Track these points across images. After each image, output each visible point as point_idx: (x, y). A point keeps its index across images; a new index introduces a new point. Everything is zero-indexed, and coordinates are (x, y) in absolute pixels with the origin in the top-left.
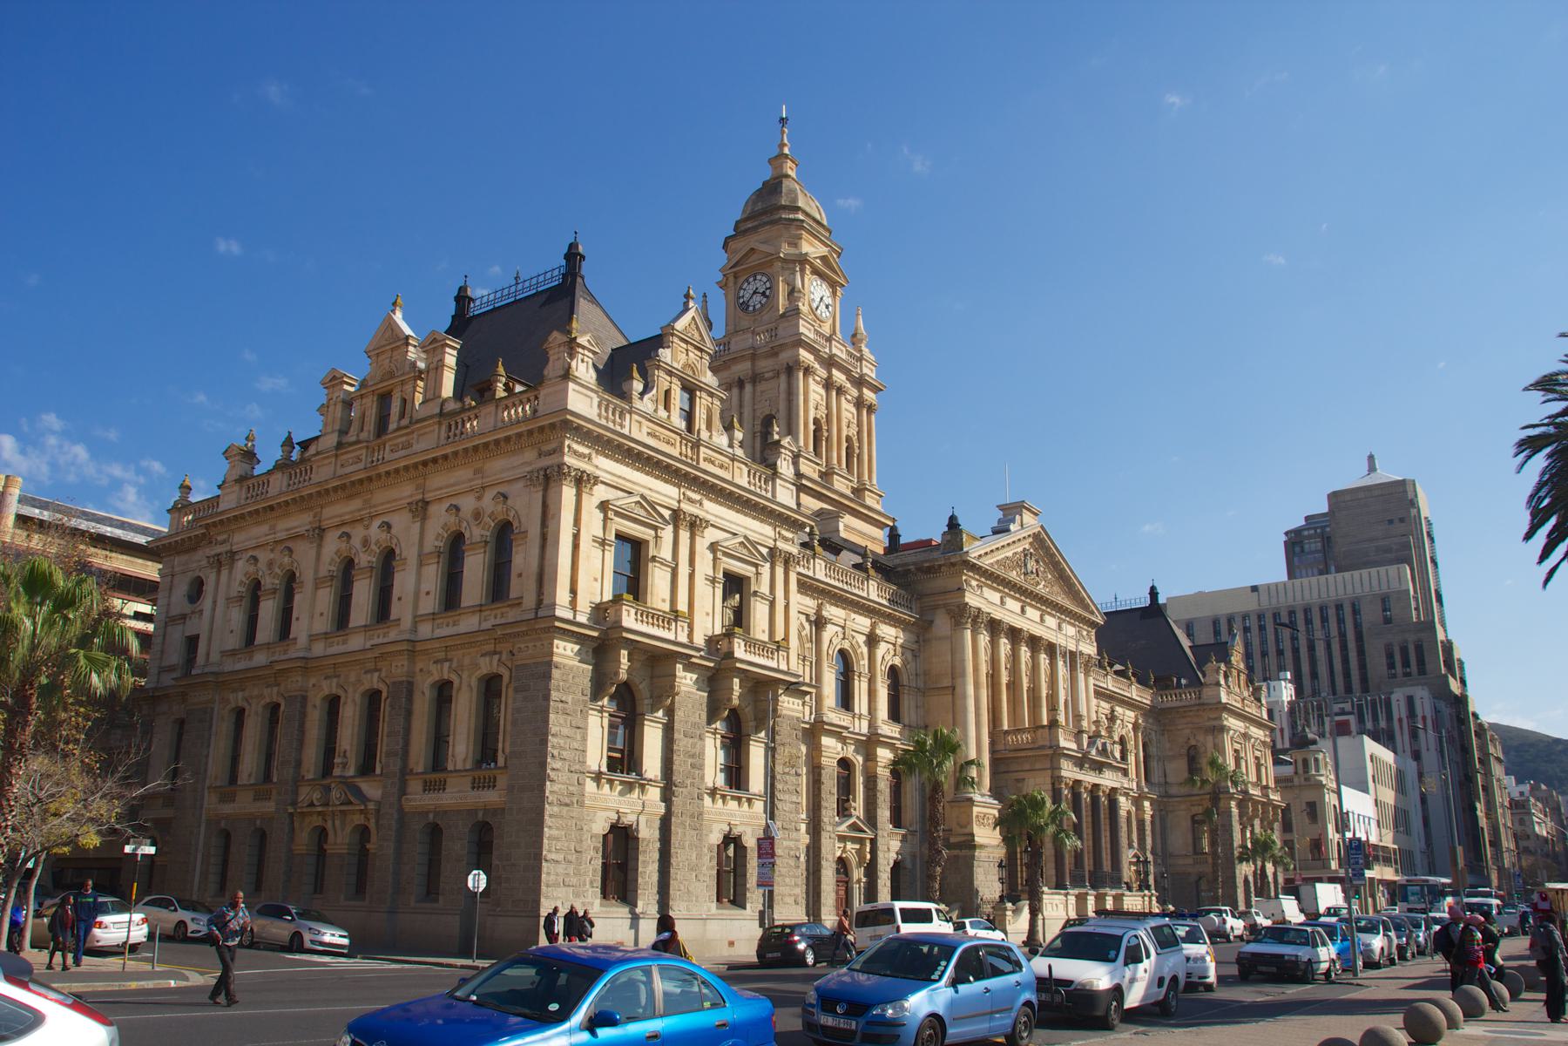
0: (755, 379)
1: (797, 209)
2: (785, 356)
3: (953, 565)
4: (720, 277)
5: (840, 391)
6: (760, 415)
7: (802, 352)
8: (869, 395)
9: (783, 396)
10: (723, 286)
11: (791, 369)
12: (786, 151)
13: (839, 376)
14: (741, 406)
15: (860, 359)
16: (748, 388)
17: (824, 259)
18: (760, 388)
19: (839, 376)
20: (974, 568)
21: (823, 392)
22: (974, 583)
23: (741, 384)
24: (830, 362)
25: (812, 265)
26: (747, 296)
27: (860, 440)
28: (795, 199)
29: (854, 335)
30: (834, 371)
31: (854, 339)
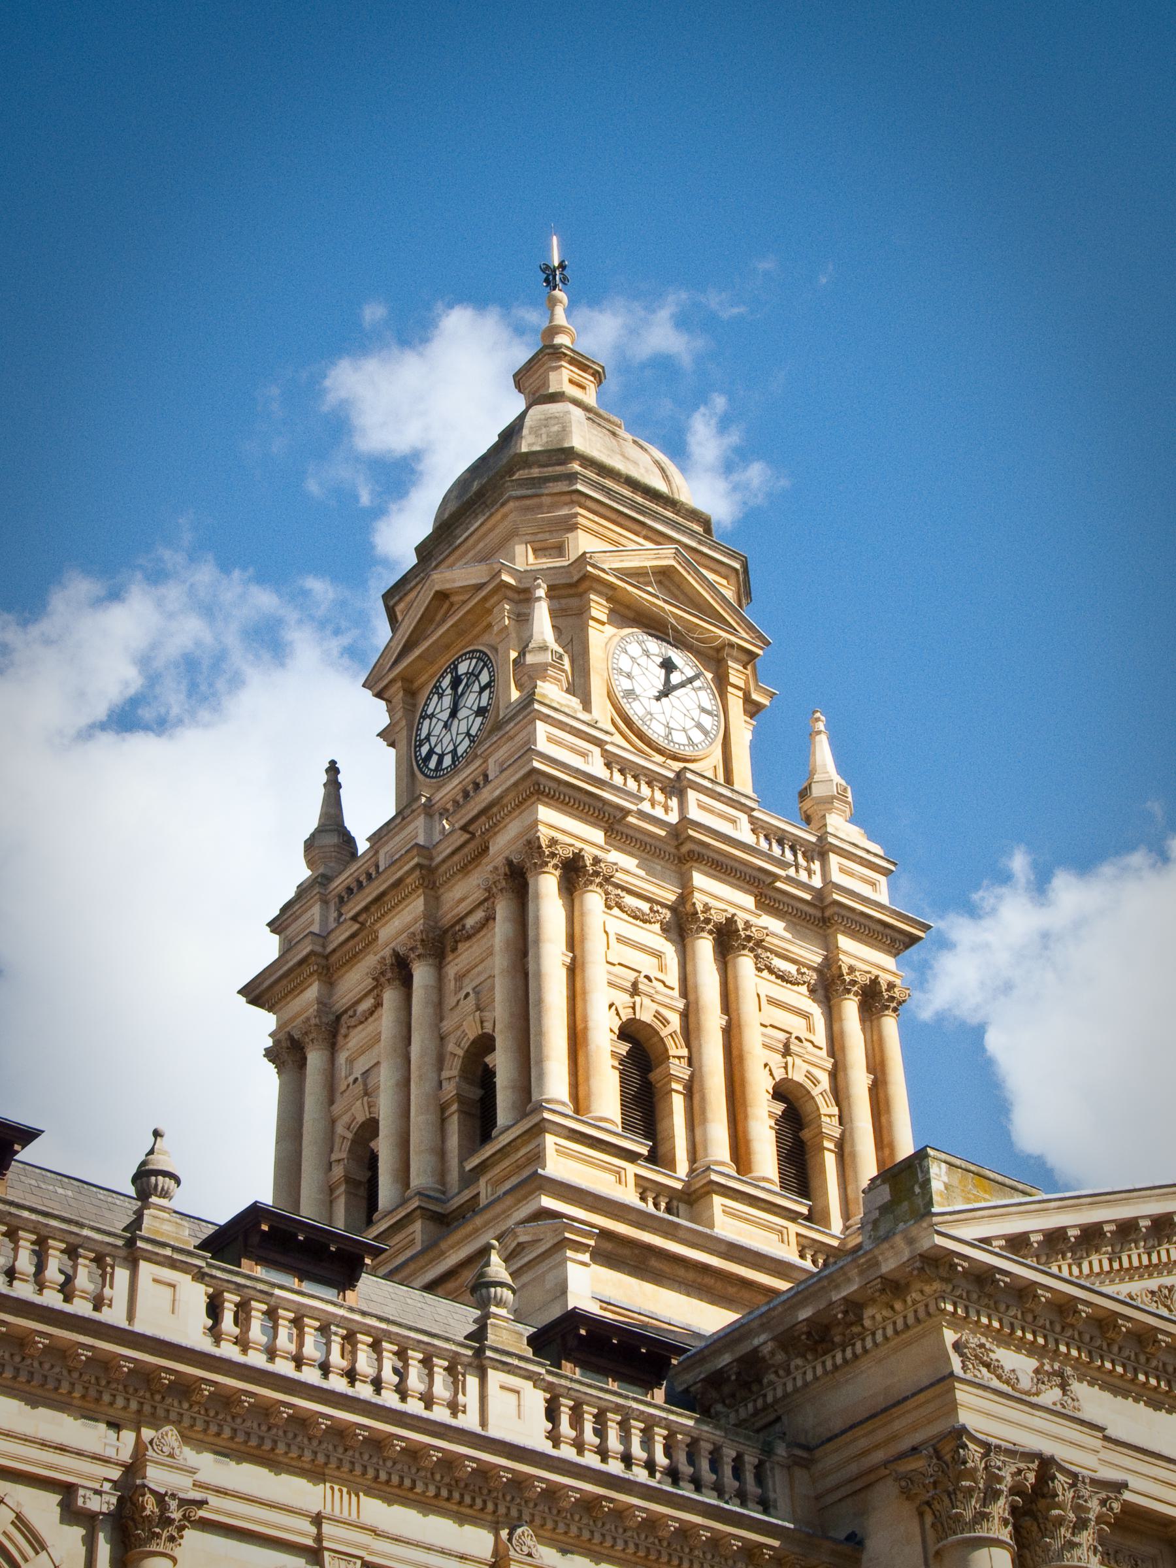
0: (440, 942)
2: (504, 844)
3: (894, 1287)
5: (728, 939)
6: (456, 1049)
8: (859, 956)
11: (518, 881)
12: (561, 339)
15: (820, 851)
16: (421, 974)
17: (665, 576)
18: (451, 971)
24: (681, 851)
25: (612, 594)
27: (839, 1092)
28: (565, 430)
29: (804, 794)
30: (699, 879)
31: (805, 802)
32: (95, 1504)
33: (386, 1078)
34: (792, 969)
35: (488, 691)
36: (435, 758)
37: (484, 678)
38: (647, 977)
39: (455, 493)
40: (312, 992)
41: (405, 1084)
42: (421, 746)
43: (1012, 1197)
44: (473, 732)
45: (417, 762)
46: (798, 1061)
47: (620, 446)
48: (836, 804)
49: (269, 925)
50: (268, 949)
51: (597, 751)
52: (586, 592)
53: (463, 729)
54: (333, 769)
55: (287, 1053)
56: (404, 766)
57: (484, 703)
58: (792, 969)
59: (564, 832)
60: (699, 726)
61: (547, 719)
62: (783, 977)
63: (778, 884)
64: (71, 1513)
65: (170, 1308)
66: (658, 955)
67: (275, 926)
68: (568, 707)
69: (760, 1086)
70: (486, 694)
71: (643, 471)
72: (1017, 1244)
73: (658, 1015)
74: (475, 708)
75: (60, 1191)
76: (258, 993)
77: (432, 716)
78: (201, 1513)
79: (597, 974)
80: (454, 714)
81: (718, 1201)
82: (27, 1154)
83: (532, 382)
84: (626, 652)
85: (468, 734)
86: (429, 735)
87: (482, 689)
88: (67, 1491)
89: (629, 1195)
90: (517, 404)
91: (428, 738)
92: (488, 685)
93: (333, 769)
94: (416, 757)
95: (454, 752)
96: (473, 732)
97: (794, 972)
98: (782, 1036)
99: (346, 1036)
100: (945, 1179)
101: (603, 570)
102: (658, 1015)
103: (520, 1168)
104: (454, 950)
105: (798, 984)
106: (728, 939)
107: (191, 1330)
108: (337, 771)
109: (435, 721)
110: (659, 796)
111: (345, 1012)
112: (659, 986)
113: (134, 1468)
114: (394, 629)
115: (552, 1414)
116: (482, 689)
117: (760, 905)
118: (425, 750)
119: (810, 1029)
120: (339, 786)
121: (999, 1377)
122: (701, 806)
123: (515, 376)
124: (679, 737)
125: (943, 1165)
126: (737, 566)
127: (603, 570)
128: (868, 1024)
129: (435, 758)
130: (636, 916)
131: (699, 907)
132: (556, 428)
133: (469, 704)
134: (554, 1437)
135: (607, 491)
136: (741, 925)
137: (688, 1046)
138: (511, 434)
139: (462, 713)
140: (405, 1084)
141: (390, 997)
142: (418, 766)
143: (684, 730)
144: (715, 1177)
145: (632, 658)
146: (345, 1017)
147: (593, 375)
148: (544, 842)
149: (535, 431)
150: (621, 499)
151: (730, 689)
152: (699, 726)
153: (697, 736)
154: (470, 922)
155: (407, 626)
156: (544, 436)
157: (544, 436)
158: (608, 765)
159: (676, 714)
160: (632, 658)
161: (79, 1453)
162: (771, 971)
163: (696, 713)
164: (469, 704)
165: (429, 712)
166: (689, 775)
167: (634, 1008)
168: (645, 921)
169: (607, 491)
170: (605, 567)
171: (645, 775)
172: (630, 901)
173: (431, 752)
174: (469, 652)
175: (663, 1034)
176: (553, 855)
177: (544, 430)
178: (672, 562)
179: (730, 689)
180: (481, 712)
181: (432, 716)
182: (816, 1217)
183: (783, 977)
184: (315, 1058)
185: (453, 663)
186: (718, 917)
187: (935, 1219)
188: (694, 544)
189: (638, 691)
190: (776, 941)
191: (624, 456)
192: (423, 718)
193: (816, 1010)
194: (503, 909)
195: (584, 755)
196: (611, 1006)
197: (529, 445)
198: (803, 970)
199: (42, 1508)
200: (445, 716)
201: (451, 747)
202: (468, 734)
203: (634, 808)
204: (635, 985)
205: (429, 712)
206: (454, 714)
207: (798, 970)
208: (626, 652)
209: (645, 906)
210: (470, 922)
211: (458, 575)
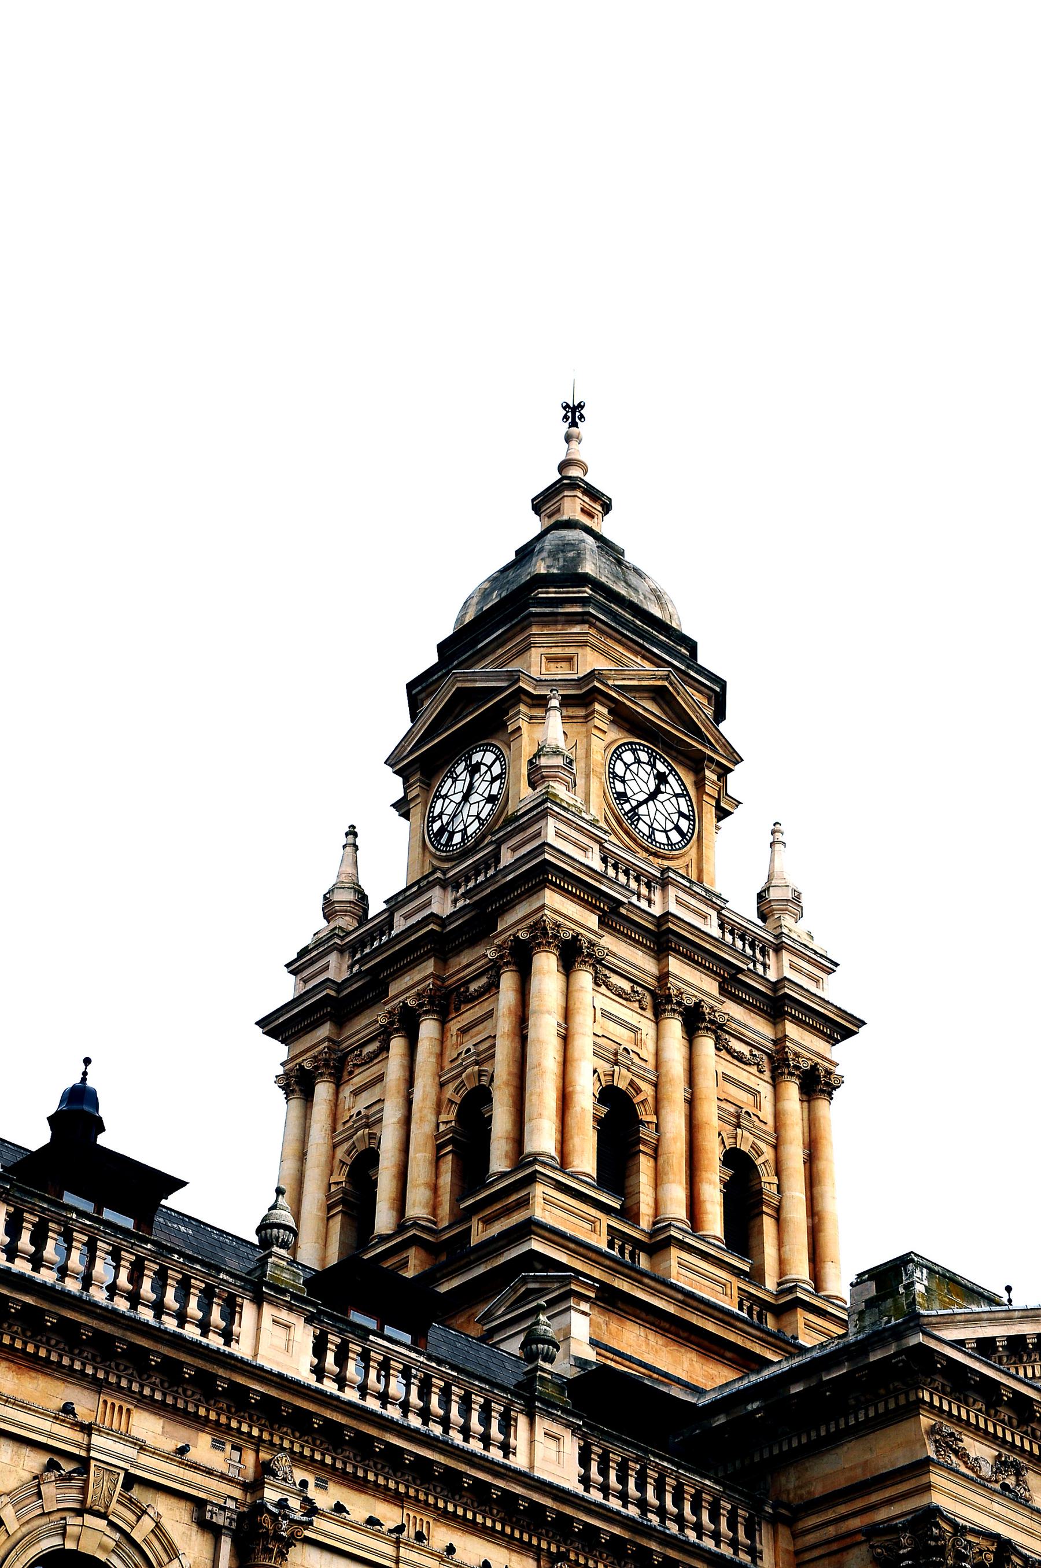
0: (445, 1002)
1: (585, 579)
2: (513, 922)
4: (395, 788)
7: (552, 899)
9: (504, 1025)
10: (402, 807)
13: (691, 980)
14: (410, 1082)
16: (428, 1029)
17: (660, 695)
18: (454, 1026)
19: (691, 980)
20: (959, 1381)
21: (647, 1027)
22: (978, 1449)
23: (407, 1024)
26: (449, 810)
28: (578, 559)
30: (675, 965)
32: (220, 1520)
33: (392, 1114)
34: (745, 1050)
35: (499, 781)
36: (446, 834)
37: (496, 770)
38: (625, 1049)
39: (475, 600)
40: (325, 1031)
41: (407, 1121)
42: (434, 821)
43: (979, 1305)
44: (483, 816)
45: (429, 836)
46: (746, 1134)
47: (623, 573)
48: (791, 907)
49: (287, 966)
50: (283, 989)
51: (596, 847)
52: (591, 703)
53: (474, 811)
54: (352, 832)
55: (298, 1083)
56: (419, 836)
57: (494, 792)
58: (745, 1050)
59: (565, 916)
60: (677, 828)
61: (557, 816)
62: (739, 1058)
63: (740, 976)
64: (205, 1525)
65: (278, 1343)
66: (635, 1030)
67: (295, 968)
68: (575, 806)
69: (713, 1152)
70: (496, 785)
71: (641, 597)
72: (985, 1347)
73: (632, 1083)
74: (486, 795)
75: (183, 1229)
76: (278, 1025)
77: (445, 797)
78: (307, 1533)
79: (584, 1045)
80: (466, 798)
81: (675, 1253)
82: (174, 1201)
83: (549, 507)
84: (622, 760)
85: (478, 817)
86: (441, 813)
87: (494, 780)
88: (199, 1504)
89: (601, 1242)
90: (534, 526)
91: (440, 816)
92: (499, 777)
93: (352, 832)
94: (428, 831)
95: (464, 831)
96: (483, 816)
97: (747, 1053)
98: (732, 1109)
99: (351, 1073)
100: (926, 1283)
101: (607, 685)
102: (632, 1083)
103: (508, 1211)
104: (457, 1009)
105: (750, 1064)
106: (695, 1021)
107: (299, 1366)
108: (355, 835)
109: (447, 801)
110: (644, 891)
111: (353, 1051)
112: (636, 1060)
113: (254, 1487)
114: (414, 716)
115: (584, 1460)
116: (494, 780)
117: (722, 991)
118: (437, 826)
119: (758, 1105)
120: (356, 847)
121: (965, 1463)
122: (679, 902)
123: (533, 500)
124: (661, 837)
125: (925, 1270)
126: (718, 689)
127: (607, 685)
128: (805, 1104)
129: (446, 834)
130: (620, 994)
131: (674, 992)
132: (571, 554)
133: (480, 791)
134: (585, 1480)
135: (614, 616)
136: (707, 1011)
137: (657, 1112)
138: (525, 553)
139: (474, 798)
140: (407, 1121)
141: (397, 1045)
142: (430, 839)
143: (666, 832)
144: (674, 1233)
145: (625, 764)
146: (353, 1055)
147: (602, 505)
148: (549, 925)
149: (553, 554)
150: (625, 623)
151: (705, 798)
152: (677, 828)
153: (675, 837)
154: (473, 987)
155: (428, 717)
156: (561, 560)
157: (561, 560)
158: (604, 860)
159: (659, 817)
160: (625, 764)
161: (209, 1472)
162: (730, 1051)
163: (675, 817)
164: (480, 791)
165: (442, 793)
166: (671, 874)
167: (613, 1075)
168: (626, 999)
169: (614, 616)
170: (610, 683)
171: (634, 870)
172: (615, 980)
173: (443, 829)
174: (483, 745)
175: (635, 1101)
176: (555, 937)
177: (561, 555)
178: (666, 684)
179: (705, 798)
180: (491, 799)
181: (445, 797)
182: (756, 1276)
183: (739, 1058)
184: (323, 1091)
185: (468, 752)
186: (689, 1002)
187: (925, 1321)
188: (683, 668)
189: (629, 794)
190: (734, 1026)
191: (626, 582)
192: (438, 797)
193: (765, 1090)
194: (508, 982)
195: (585, 850)
196: (595, 1071)
197: (548, 567)
198: (755, 1052)
199: (175, 1519)
200: (458, 798)
201: (461, 827)
202: (478, 817)
203: (626, 900)
204: (616, 1054)
205: (442, 793)
206: (466, 798)
207: (751, 1051)
208: (622, 760)
209: (626, 986)
210: (473, 987)
211: (482, 674)
